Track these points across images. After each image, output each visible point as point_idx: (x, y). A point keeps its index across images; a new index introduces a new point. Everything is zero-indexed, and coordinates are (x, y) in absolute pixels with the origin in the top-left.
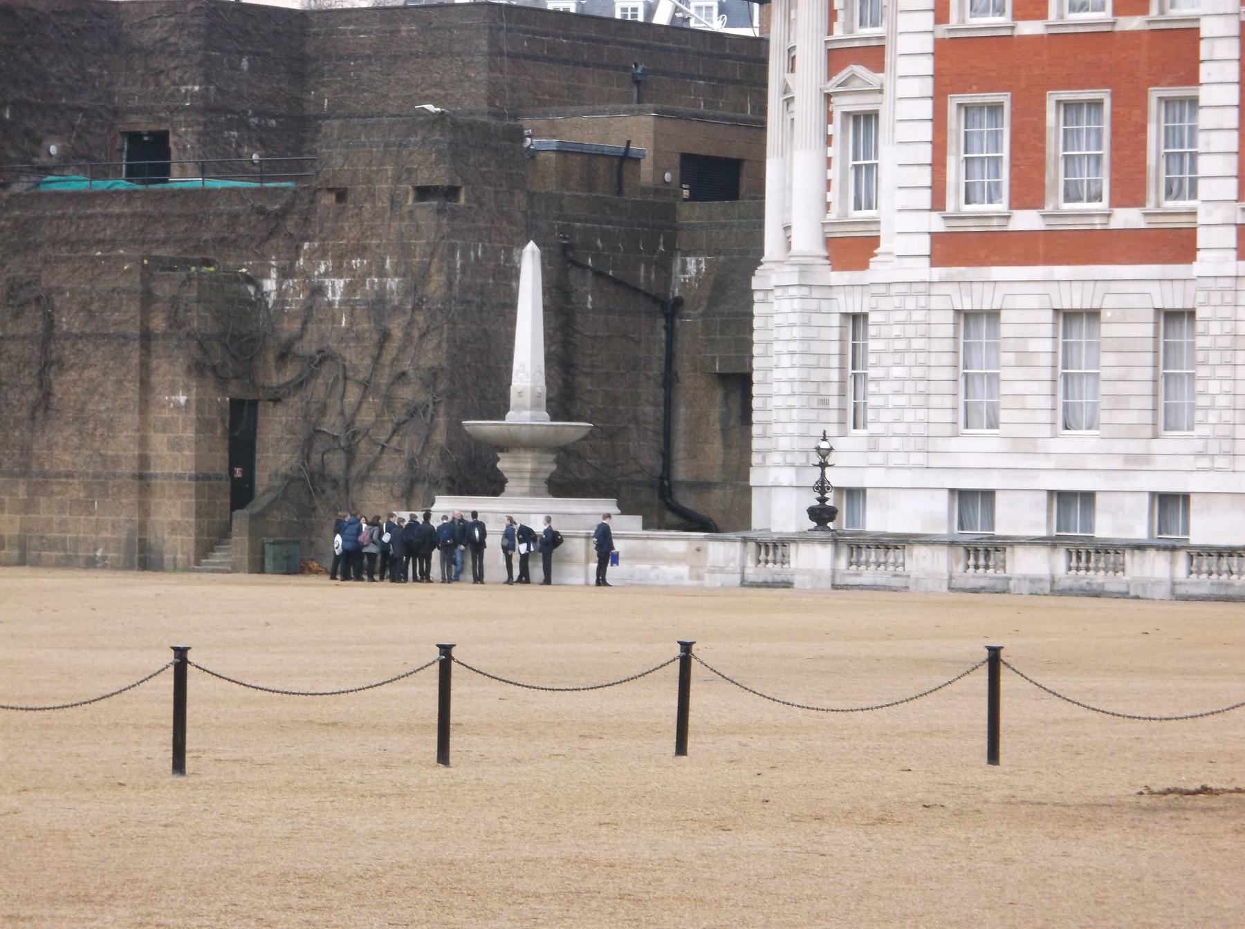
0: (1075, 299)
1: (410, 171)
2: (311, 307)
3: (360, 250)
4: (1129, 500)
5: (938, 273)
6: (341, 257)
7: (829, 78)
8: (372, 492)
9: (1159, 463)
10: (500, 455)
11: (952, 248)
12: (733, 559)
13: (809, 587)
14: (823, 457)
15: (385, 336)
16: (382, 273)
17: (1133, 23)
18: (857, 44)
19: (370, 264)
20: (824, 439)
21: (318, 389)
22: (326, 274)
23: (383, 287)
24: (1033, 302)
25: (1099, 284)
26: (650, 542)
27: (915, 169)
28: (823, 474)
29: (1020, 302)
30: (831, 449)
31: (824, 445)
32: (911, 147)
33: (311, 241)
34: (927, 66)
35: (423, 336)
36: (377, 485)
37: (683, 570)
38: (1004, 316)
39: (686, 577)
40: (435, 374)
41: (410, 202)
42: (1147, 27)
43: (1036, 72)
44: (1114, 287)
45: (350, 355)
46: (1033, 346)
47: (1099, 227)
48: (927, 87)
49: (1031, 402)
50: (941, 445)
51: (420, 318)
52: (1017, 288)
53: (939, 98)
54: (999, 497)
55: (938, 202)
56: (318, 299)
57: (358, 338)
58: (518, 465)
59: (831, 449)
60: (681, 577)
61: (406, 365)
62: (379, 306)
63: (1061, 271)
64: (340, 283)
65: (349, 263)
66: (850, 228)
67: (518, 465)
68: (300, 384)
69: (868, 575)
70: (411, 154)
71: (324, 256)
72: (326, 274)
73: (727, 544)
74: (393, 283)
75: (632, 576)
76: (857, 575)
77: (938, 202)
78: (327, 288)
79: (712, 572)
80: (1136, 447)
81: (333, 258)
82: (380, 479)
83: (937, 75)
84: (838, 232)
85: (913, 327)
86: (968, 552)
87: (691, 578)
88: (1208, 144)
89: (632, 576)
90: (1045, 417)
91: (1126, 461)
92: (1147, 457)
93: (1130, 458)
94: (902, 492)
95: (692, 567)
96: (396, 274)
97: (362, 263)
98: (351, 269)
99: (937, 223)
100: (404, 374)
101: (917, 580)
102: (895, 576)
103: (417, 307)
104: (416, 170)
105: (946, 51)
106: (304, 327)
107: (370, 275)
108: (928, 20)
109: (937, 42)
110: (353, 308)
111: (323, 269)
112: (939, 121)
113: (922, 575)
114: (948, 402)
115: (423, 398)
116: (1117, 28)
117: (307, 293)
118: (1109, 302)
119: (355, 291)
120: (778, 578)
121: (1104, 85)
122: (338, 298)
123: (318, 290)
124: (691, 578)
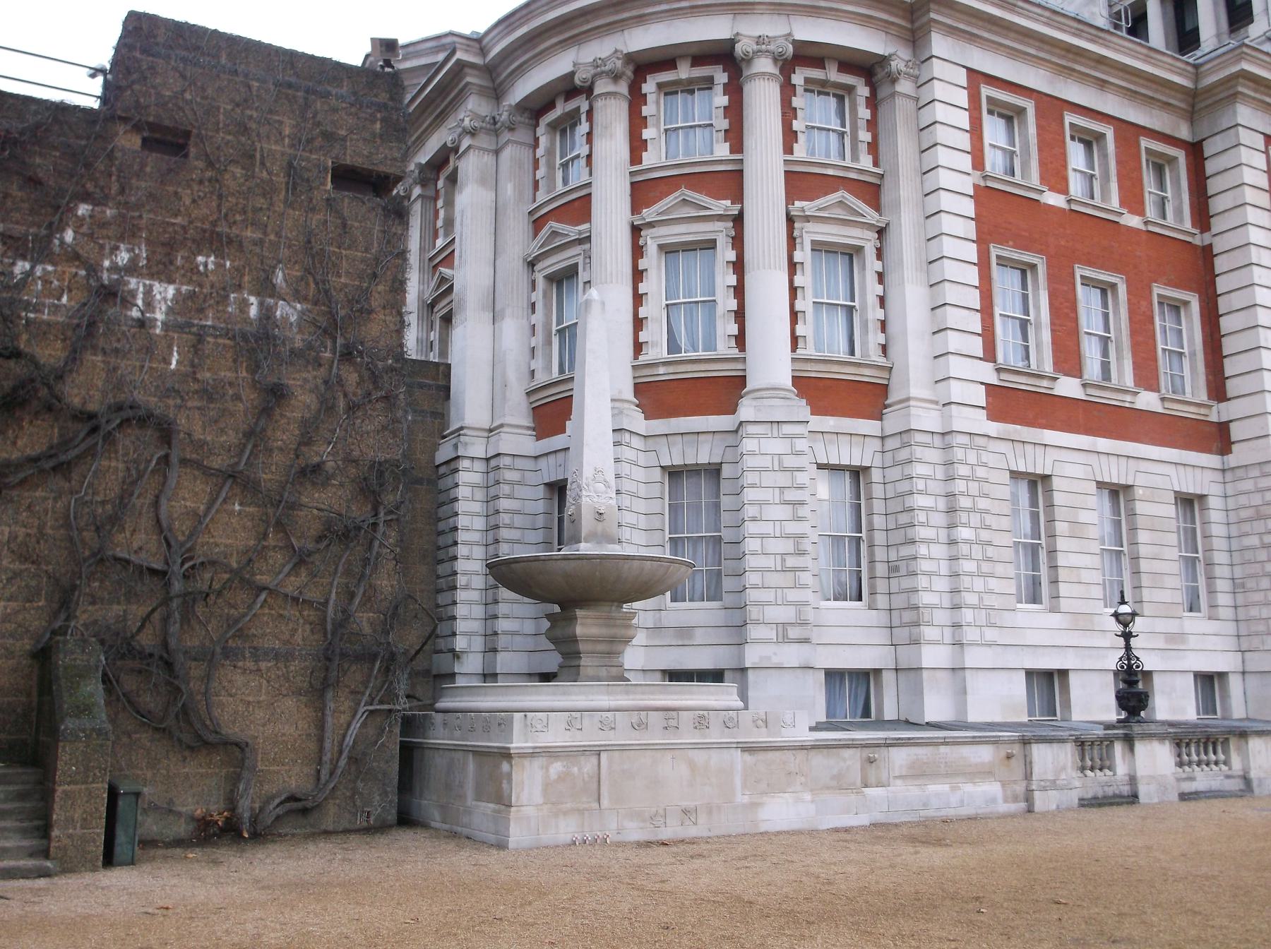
0: (1115, 474)
1: (329, 137)
2: (92, 324)
3: (214, 242)
4: (1178, 677)
5: (994, 428)
6: (171, 246)
7: (536, 235)
8: (239, 679)
9: (1193, 642)
10: (579, 613)
11: (1008, 403)
12: (1064, 768)
13: (1156, 800)
14: (1126, 625)
15: (276, 394)
16: (265, 288)
17: (1133, 221)
18: (830, 172)
19: (239, 271)
20: (1123, 602)
21: (108, 472)
22: (132, 269)
23: (267, 314)
24: (1079, 471)
25: (1131, 461)
26: (943, 749)
27: (967, 312)
28: (1128, 647)
29: (1070, 470)
30: (1134, 614)
31: (1125, 609)
32: (960, 287)
33: (96, 203)
34: (969, 208)
35: (352, 408)
36: (250, 664)
37: (992, 788)
38: (1056, 483)
39: (1000, 800)
40: (381, 474)
41: (329, 186)
42: (1142, 227)
43: (1063, 243)
44: (1144, 466)
45: (191, 422)
46: (1084, 517)
47: (1127, 405)
48: (970, 229)
49: (1086, 576)
50: (1007, 618)
51: (351, 377)
52: (1064, 455)
53: (982, 241)
54: (1073, 678)
55: (990, 353)
56: (112, 311)
57: (208, 394)
58: (612, 631)
59: (1134, 614)
60: (994, 800)
61: (322, 452)
62: (259, 342)
63: (1103, 444)
64: (165, 292)
65: (190, 259)
66: (835, 368)
67: (612, 631)
68: (55, 464)
69: (1204, 779)
70: (335, 110)
71: (128, 233)
72: (132, 269)
73: (1055, 745)
74: (288, 312)
75: (926, 805)
76: (1192, 779)
77: (990, 353)
78: (133, 294)
79: (1044, 789)
80: (1171, 626)
81: (149, 242)
82: (257, 654)
83: (978, 219)
84: (813, 371)
85: (976, 484)
86: (1178, 745)
87: (1006, 801)
88: (1266, 340)
89: (926, 805)
90: (1097, 592)
91: (1167, 641)
92: (1180, 637)
93: (1172, 637)
94: (980, 673)
95: (1003, 785)
96: (298, 296)
97: (219, 266)
98: (194, 269)
99: (988, 373)
100: (317, 468)
101: (1260, 780)
102: (1228, 777)
103: (347, 355)
104: (344, 139)
105: (985, 196)
106: (74, 357)
107: (239, 287)
108: (966, 162)
109: (976, 187)
110: (200, 338)
111: (123, 257)
112: (983, 265)
113: (1262, 775)
114: (1011, 571)
115: (359, 512)
116: (1122, 222)
117: (81, 296)
118: (1140, 480)
119: (201, 310)
120: (1110, 791)
121: (1117, 270)
122: (160, 316)
123: (112, 294)
124: (1006, 801)
